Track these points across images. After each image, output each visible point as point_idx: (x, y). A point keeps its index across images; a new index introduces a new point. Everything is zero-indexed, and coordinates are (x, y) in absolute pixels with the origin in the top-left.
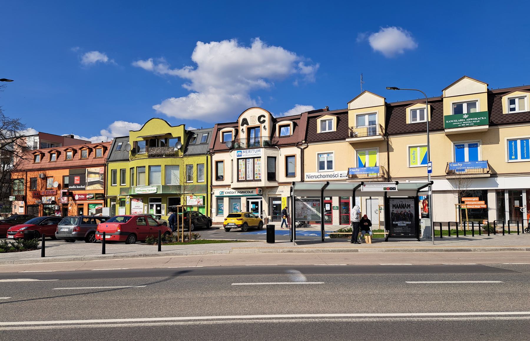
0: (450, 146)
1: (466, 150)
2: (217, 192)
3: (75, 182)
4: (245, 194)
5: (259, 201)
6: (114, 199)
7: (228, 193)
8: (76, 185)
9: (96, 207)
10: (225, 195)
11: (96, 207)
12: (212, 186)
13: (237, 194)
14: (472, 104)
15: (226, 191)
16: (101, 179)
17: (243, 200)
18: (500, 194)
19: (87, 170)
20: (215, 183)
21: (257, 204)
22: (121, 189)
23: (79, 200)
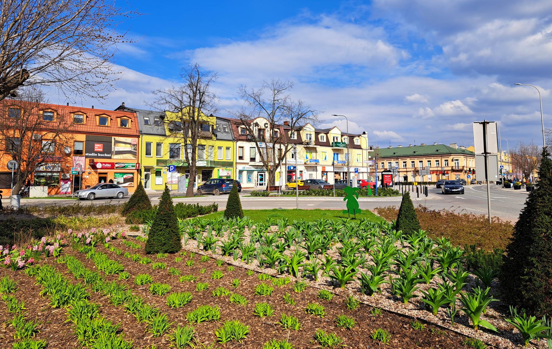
0: (333, 153)
1: (336, 155)
2: (240, 167)
3: (96, 149)
4: (258, 169)
5: (263, 173)
6: (147, 169)
7: (249, 168)
8: (97, 152)
9: (125, 176)
10: (246, 169)
11: (125, 176)
12: (236, 163)
13: (253, 169)
14: (337, 139)
15: (247, 167)
16: (133, 149)
17: (255, 173)
18: (343, 173)
19: (114, 139)
20: (238, 161)
21: (262, 175)
22: (157, 160)
23: (102, 168)
